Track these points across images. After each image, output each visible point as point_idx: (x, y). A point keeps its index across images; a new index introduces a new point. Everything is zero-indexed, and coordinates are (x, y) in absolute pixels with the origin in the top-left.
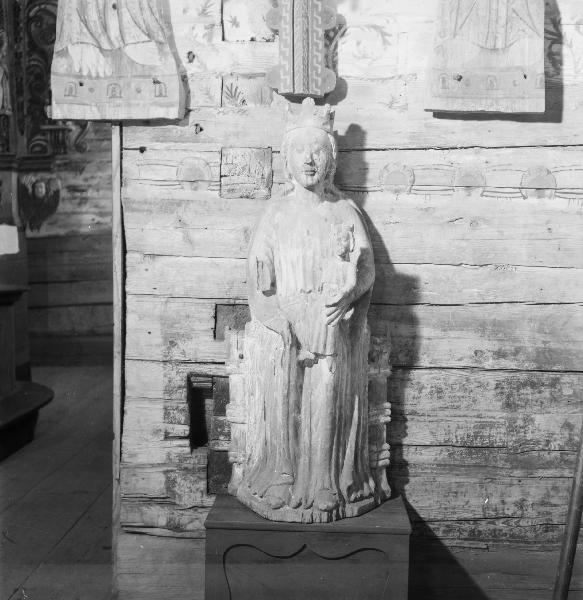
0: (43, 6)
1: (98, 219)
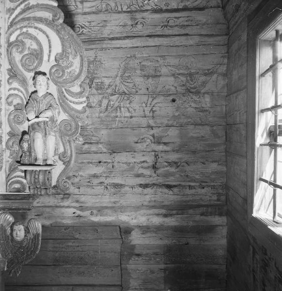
0: (24, 30)
1: (78, 212)
